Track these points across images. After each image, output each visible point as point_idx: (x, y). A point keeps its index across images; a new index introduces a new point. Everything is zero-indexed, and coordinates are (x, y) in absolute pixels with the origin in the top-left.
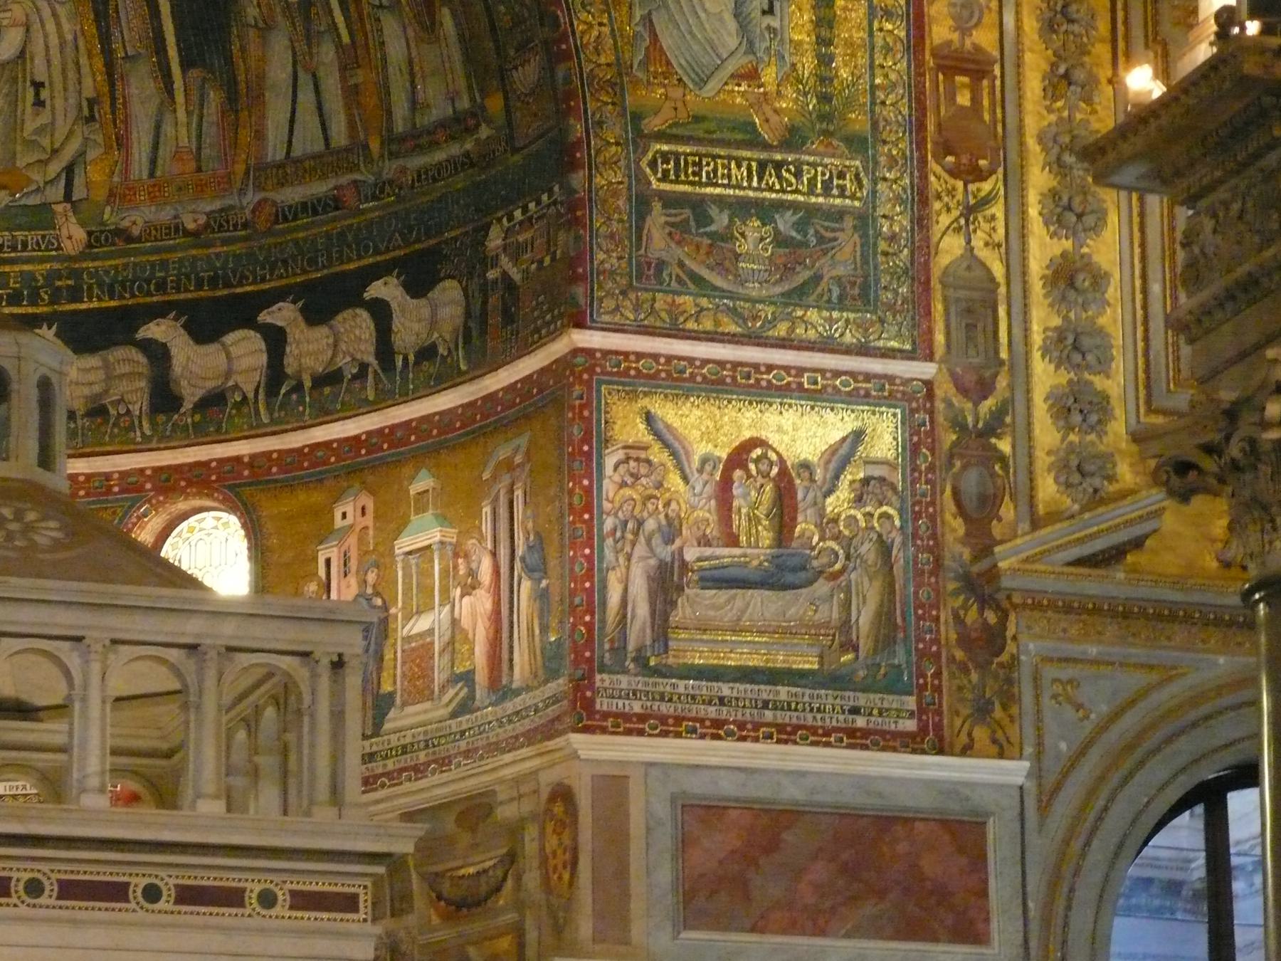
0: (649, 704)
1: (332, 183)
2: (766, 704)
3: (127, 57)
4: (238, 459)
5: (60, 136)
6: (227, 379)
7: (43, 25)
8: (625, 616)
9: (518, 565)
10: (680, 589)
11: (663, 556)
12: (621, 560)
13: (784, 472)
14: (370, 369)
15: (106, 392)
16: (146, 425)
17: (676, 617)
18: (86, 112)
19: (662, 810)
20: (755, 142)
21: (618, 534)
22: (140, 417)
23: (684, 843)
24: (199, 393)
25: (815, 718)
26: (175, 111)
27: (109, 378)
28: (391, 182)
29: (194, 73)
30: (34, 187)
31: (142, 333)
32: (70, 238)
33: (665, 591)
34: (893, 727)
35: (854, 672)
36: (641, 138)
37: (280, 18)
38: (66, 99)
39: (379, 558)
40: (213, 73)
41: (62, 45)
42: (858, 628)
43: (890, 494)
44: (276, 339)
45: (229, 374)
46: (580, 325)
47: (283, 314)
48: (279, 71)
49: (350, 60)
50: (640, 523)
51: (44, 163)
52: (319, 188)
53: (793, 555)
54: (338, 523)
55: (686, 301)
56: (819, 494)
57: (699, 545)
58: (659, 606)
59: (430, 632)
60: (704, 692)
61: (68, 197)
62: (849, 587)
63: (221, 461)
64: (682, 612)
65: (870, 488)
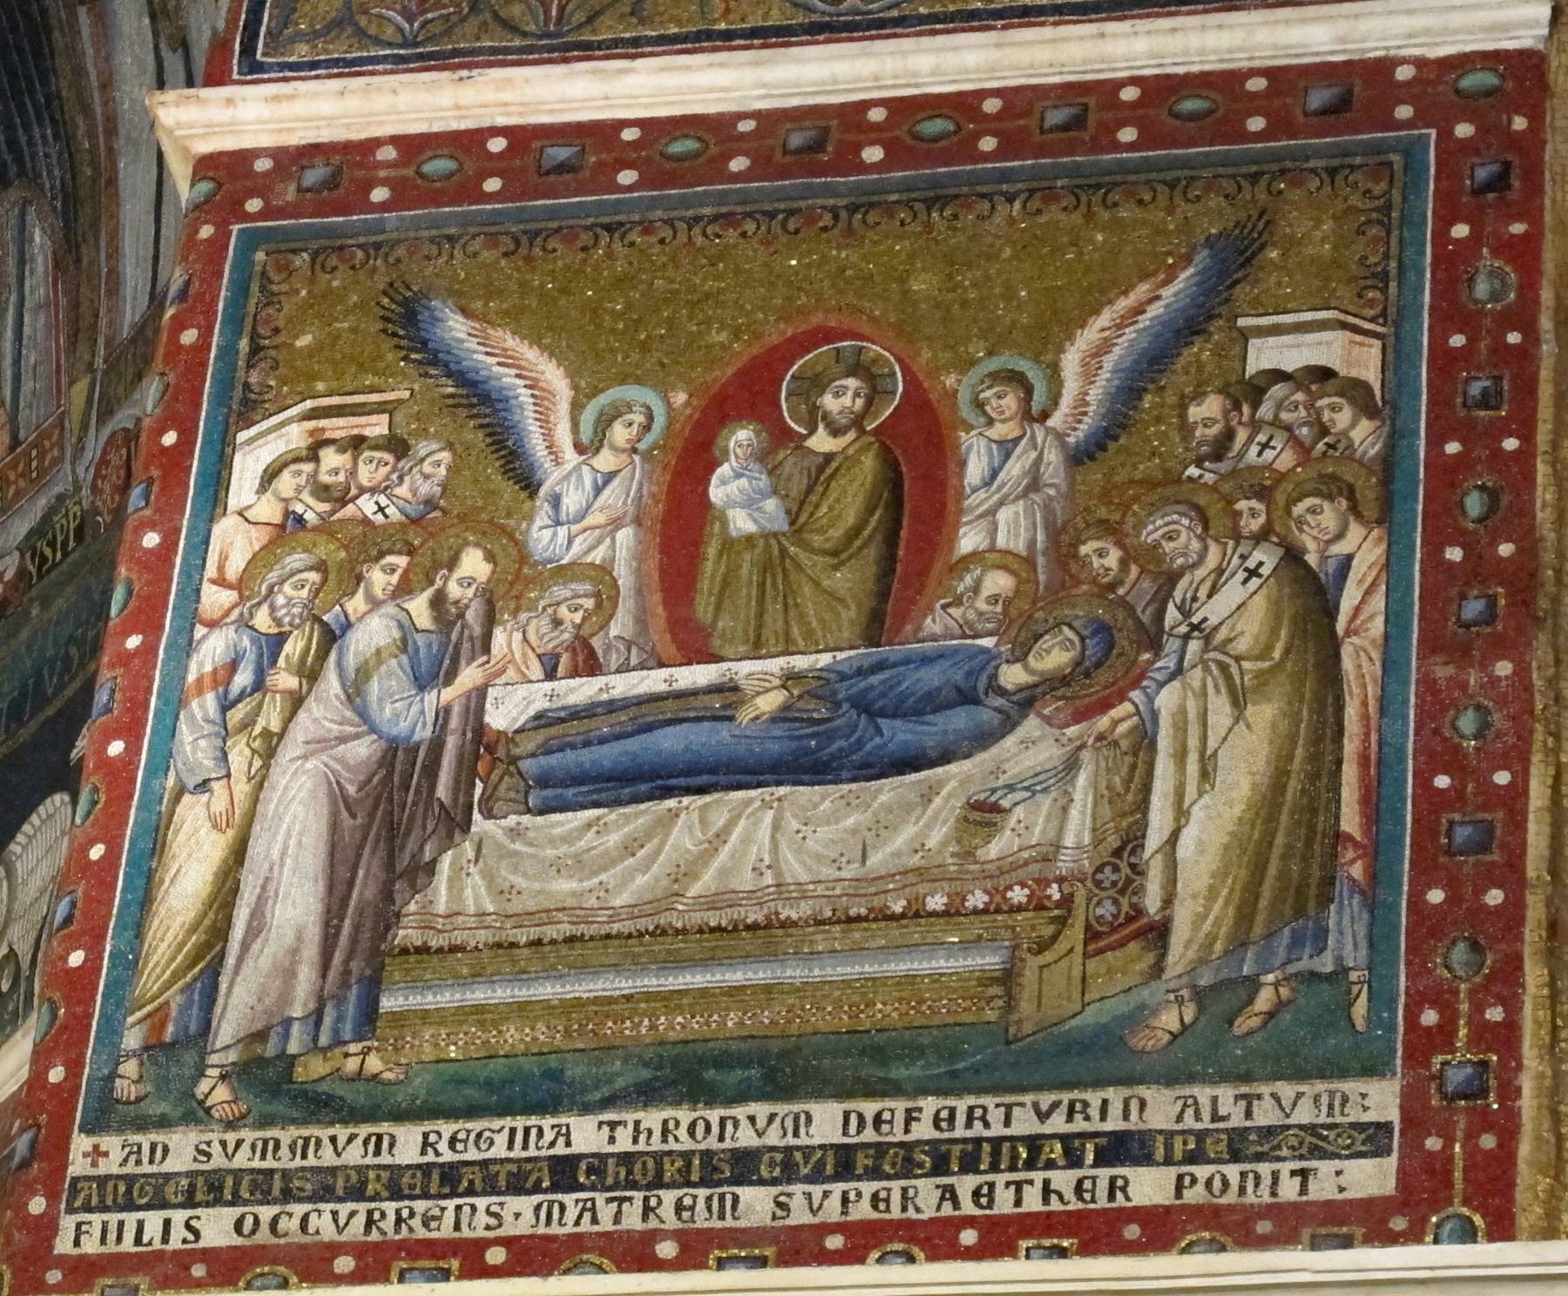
0: (266, 1213)
2: (745, 1166)
8: (219, 933)
10: (456, 823)
11: (403, 727)
12: (239, 755)
21: (243, 678)
25: (949, 1194)
33: (393, 834)
34: (1289, 1190)
35: (1139, 1017)
42: (1172, 866)
43: (1342, 418)
50: (331, 637)
53: (926, 660)
56: (1053, 456)
57: (550, 675)
58: (365, 889)
60: (499, 1150)
62: (1144, 740)
65: (1265, 411)
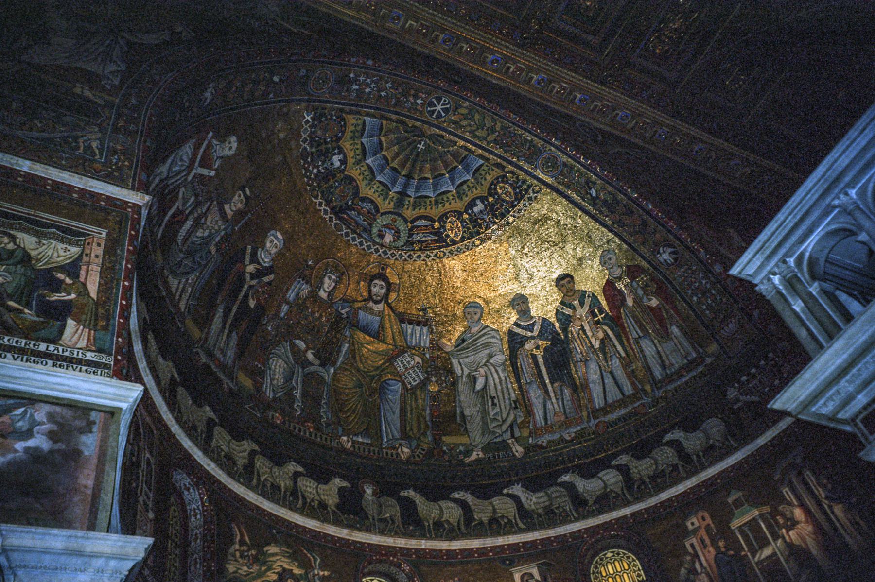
1: (630, 408)
3: (527, 383)
4: (625, 517)
5: (504, 416)
6: (606, 490)
7: (492, 376)
9: (825, 504)
14: (679, 466)
15: (551, 504)
16: (575, 514)
18: (513, 405)
22: (570, 511)
24: (594, 497)
26: (550, 399)
27: (550, 499)
28: (661, 398)
29: (556, 385)
30: (497, 435)
31: (559, 480)
32: (517, 451)
37: (591, 355)
38: (505, 402)
40: (564, 382)
41: (501, 381)
44: (624, 470)
45: (606, 486)
47: (624, 459)
48: (594, 376)
51: (501, 425)
54: (690, 527)
59: (774, 554)
61: (513, 436)
63: (617, 520)
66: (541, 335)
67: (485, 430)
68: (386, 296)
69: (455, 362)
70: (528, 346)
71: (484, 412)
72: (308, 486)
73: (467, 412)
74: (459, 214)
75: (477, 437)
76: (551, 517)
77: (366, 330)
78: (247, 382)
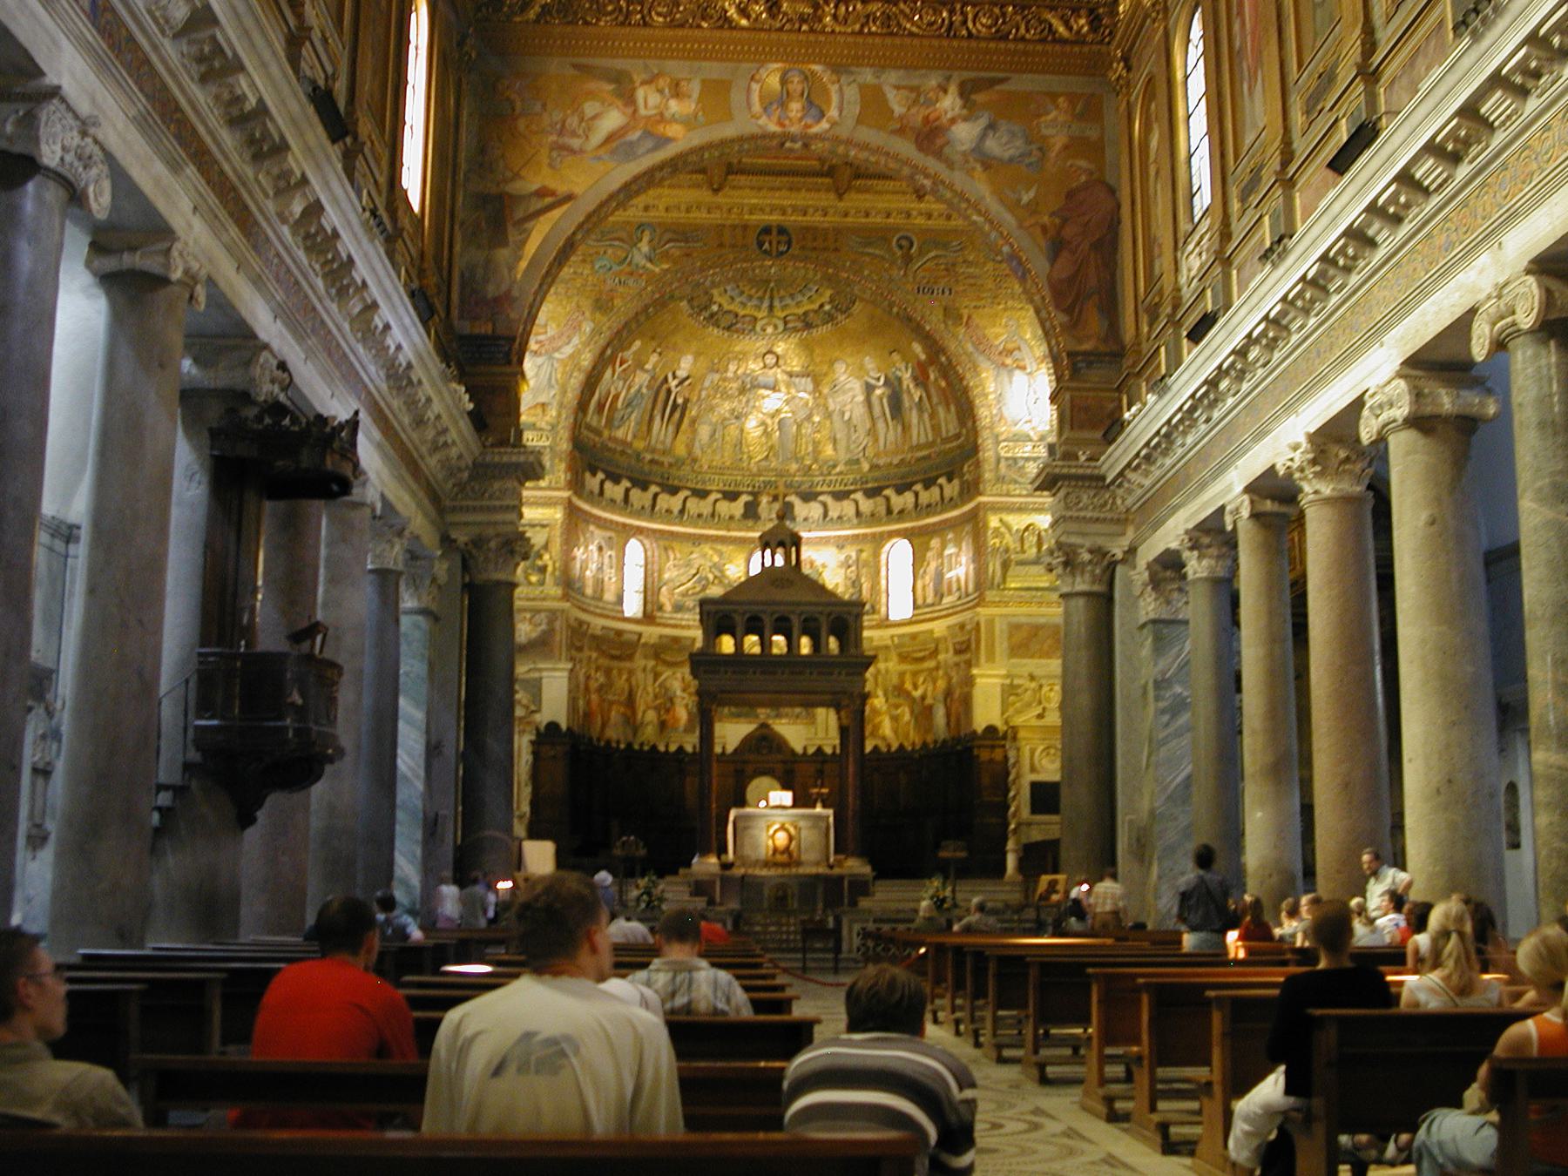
13: (1039, 535)
17: (1009, 573)
19: (1005, 627)
20: (1031, 440)
23: (1010, 636)
27: (876, 506)
36: (998, 443)
39: (940, 555)
44: (917, 495)
46: (980, 494)
47: (918, 487)
48: (915, 421)
49: (932, 416)
52: (924, 453)
55: (1012, 487)
64: (1010, 573)
66: (886, 383)
67: (848, 450)
68: (777, 364)
69: (830, 400)
70: (878, 392)
71: (849, 438)
72: (724, 507)
73: (838, 436)
74: (816, 312)
75: (843, 456)
76: (873, 519)
77: (766, 387)
78: (681, 450)
